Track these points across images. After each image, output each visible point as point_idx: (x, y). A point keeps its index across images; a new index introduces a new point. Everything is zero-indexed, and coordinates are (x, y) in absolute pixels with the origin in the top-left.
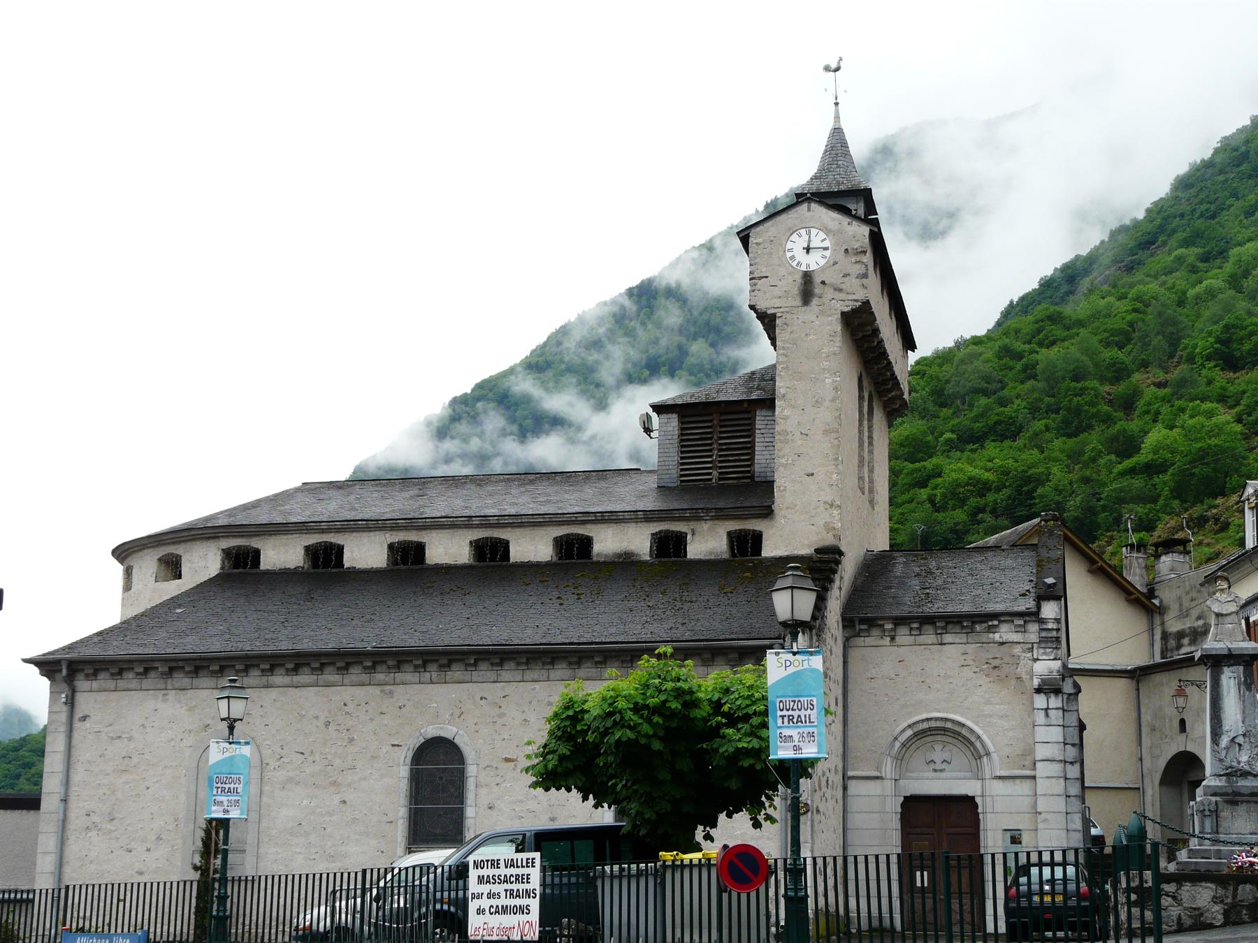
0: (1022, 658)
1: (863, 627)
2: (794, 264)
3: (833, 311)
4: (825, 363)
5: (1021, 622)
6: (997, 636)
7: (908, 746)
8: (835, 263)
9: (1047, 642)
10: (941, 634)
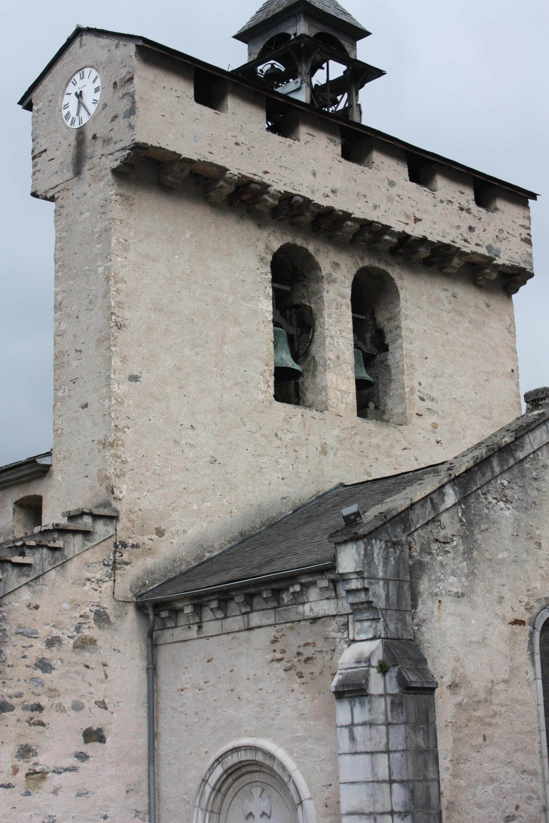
0: (338, 640)
1: (164, 614)
2: (68, 123)
3: (104, 172)
4: (98, 246)
5: (324, 583)
6: (306, 610)
7: (223, 790)
8: (105, 106)
9: (360, 611)
10: (247, 613)
